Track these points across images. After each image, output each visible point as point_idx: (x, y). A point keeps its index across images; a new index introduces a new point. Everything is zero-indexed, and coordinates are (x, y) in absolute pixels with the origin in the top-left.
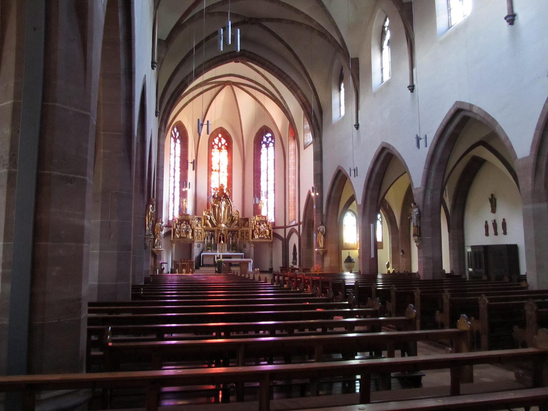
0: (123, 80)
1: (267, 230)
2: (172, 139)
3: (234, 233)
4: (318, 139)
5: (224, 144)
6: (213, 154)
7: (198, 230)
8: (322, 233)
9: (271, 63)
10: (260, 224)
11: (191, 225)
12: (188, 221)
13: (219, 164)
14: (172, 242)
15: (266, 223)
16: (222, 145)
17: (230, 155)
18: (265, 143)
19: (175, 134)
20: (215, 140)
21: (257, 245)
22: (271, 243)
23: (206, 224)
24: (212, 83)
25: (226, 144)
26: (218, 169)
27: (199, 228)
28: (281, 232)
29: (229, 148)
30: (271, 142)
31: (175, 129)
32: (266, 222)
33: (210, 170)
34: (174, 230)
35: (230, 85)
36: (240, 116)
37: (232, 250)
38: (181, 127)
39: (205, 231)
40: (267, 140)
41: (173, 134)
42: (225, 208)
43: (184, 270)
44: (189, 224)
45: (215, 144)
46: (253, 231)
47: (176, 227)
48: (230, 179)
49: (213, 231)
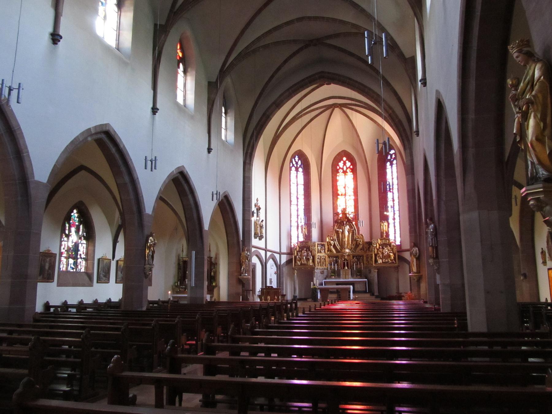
0: (6, 139)
1: (391, 254)
2: (293, 169)
3: (359, 258)
4: (408, 151)
5: (349, 167)
6: (338, 178)
7: (321, 257)
8: (414, 256)
9: (350, 79)
10: (383, 248)
11: (311, 252)
12: (308, 249)
13: (345, 187)
14: (294, 269)
15: (390, 246)
16: (347, 168)
17: (355, 178)
18: (390, 160)
19: (297, 163)
20: (340, 164)
21: (381, 271)
22: (397, 268)
23: (329, 250)
24: (317, 109)
25: (351, 167)
26: (344, 193)
27: (321, 255)
28: (407, 255)
29: (354, 171)
30: (395, 158)
31: (297, 158)
32: (390, 245)
33: (335, 194)
34: (295, 257)
35: (338, 107)
36: (358, 136)
37: (357, 275)
38: (301, 155)
39: (329, 257)
40: (391, 157)
41: (294, 163)
42: (348, 232)
43: (269, 297)
44: (309, 250)
45: (340, 168)
46: (376, 255)
47: (297, 254)
48: (356, 201)
49: (337, 257)
